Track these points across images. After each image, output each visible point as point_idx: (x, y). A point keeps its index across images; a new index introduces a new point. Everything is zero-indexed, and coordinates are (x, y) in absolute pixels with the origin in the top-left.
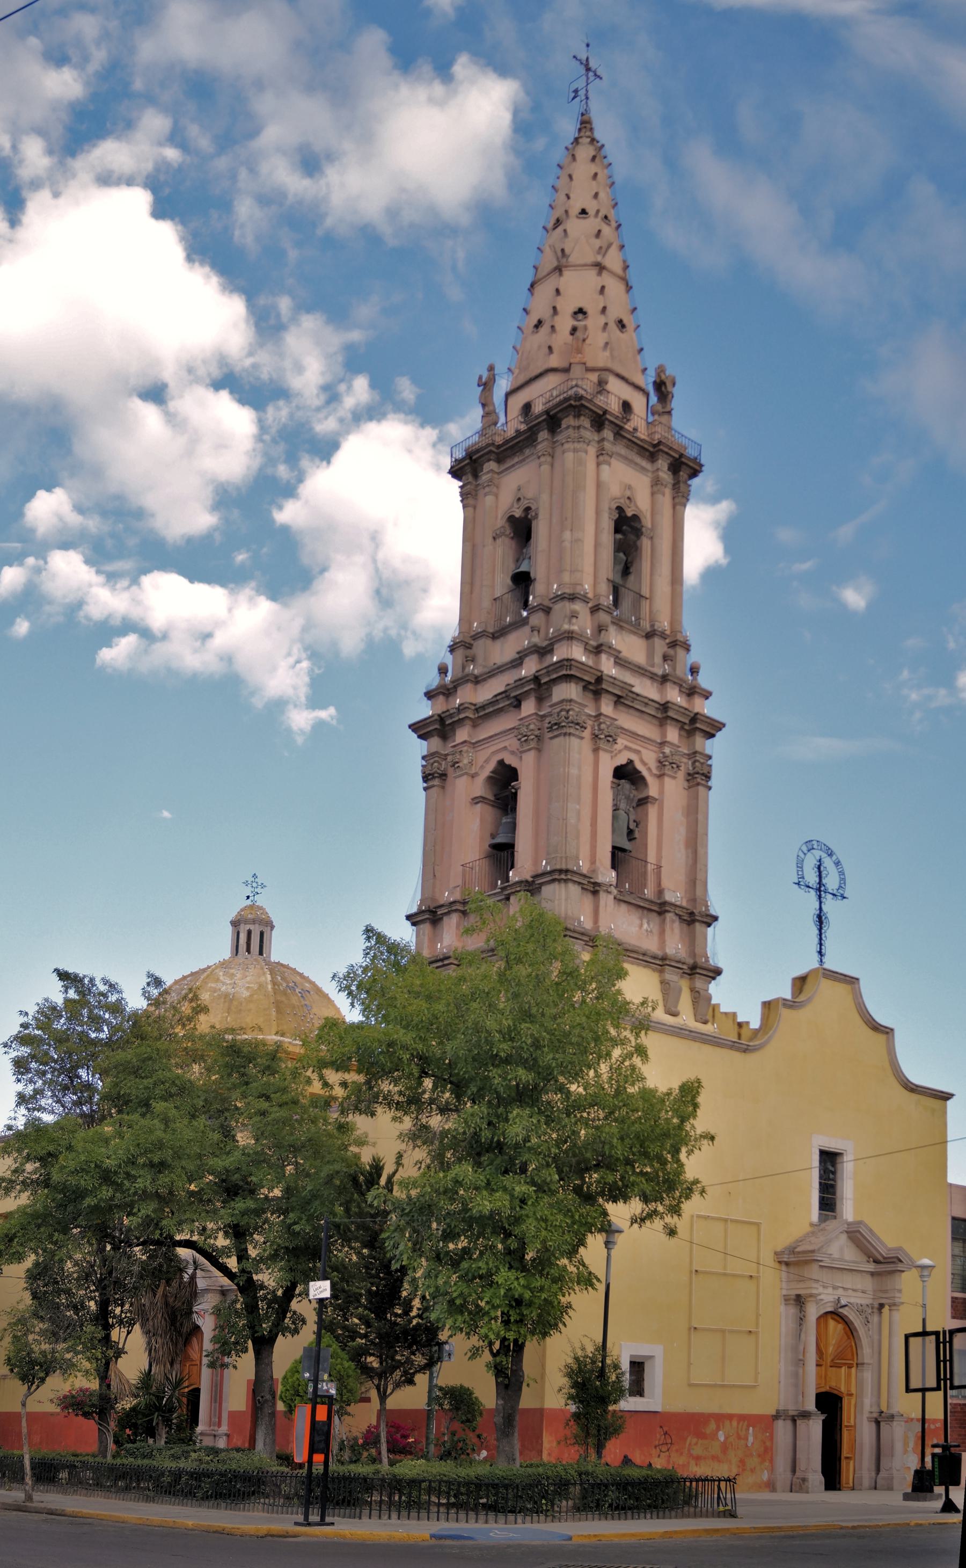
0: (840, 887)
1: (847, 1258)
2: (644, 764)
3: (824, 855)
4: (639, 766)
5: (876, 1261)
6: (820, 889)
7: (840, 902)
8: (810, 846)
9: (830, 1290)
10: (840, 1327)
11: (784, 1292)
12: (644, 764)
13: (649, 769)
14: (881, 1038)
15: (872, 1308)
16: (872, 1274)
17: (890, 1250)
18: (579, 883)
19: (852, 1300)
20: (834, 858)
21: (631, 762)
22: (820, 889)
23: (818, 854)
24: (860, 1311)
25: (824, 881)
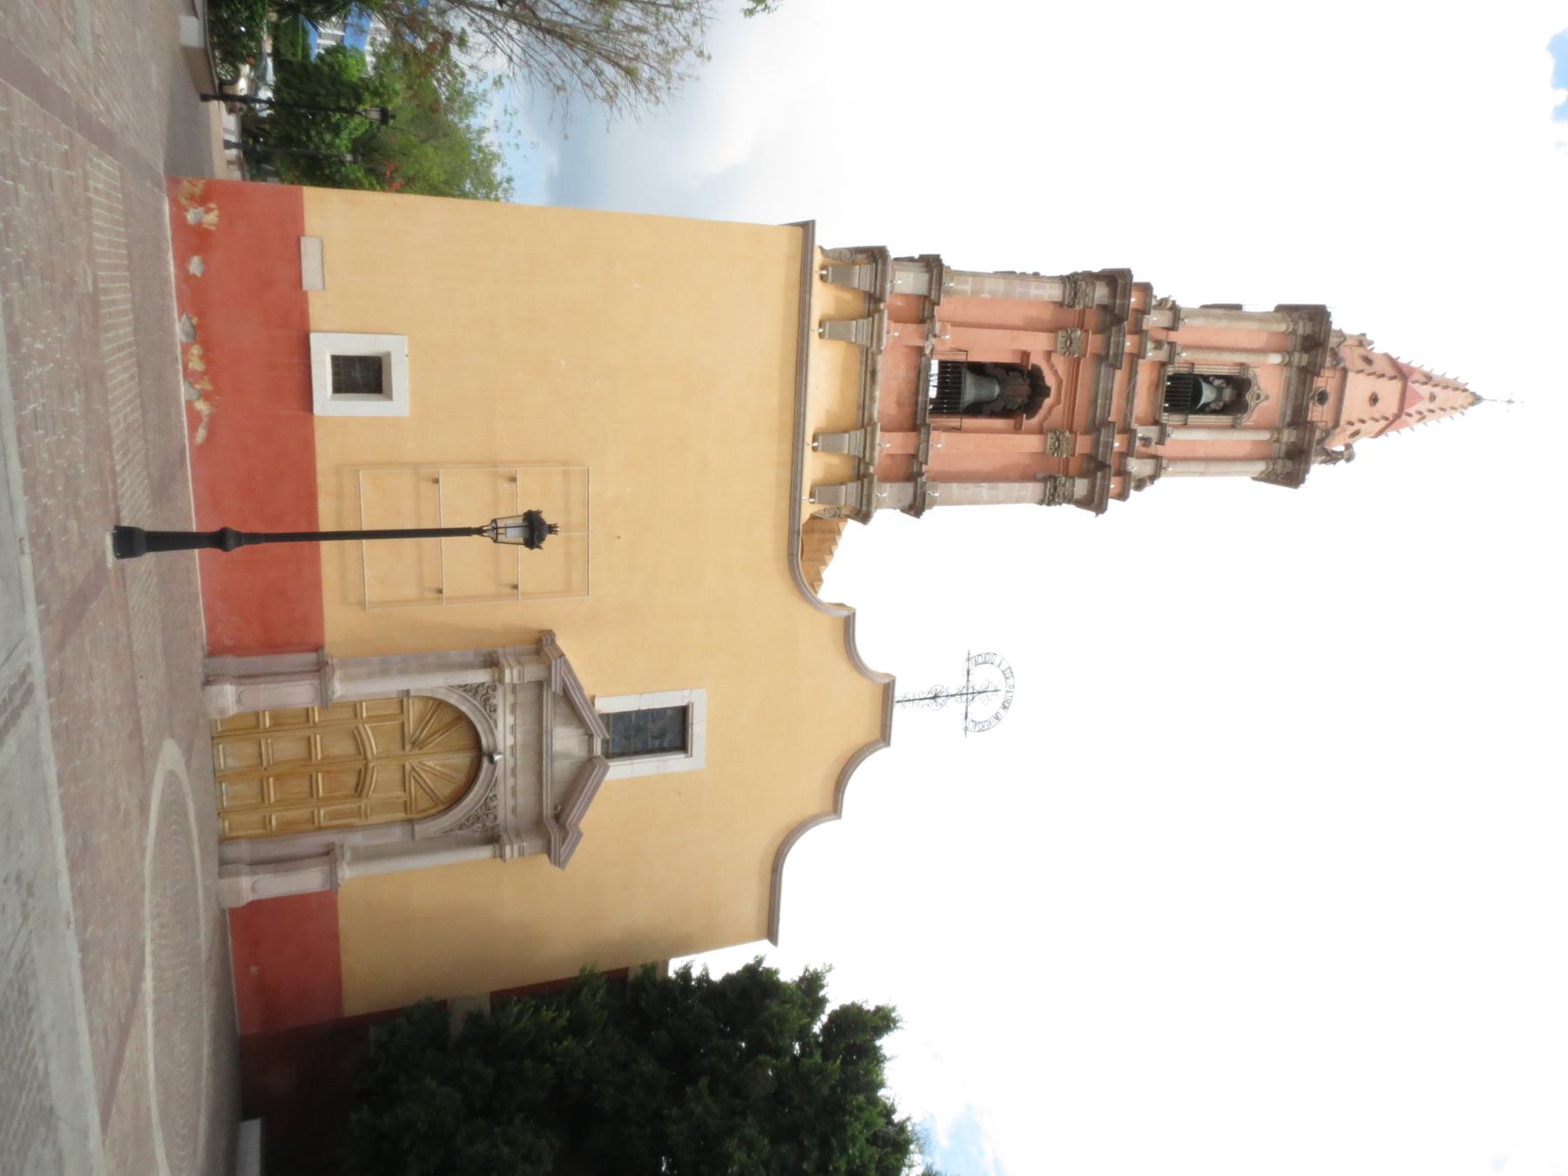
0: (976, 724)
1: (557, 764)
2: (1049, 412)
3: (1001, 695)
4: (1048, 402)
5: (557, 817)
6: (968, 694)
7: (961, 723)
8: (1008, 674)
9: (510, 741)
10: (461, 778)
11: (500, 651)
12: (1049, 412)
13: (1045, 418)
14: (829, 806)
15: (493, 828)
16: (540, 814)
17: (576, 825)
18: (930, 290)
19: (501, 787)
20: (1002, 712)
21: (1045, 392)
22: (968, 694)
23: (1002, 686)
24: (487, 805)
25: (977, 697)
